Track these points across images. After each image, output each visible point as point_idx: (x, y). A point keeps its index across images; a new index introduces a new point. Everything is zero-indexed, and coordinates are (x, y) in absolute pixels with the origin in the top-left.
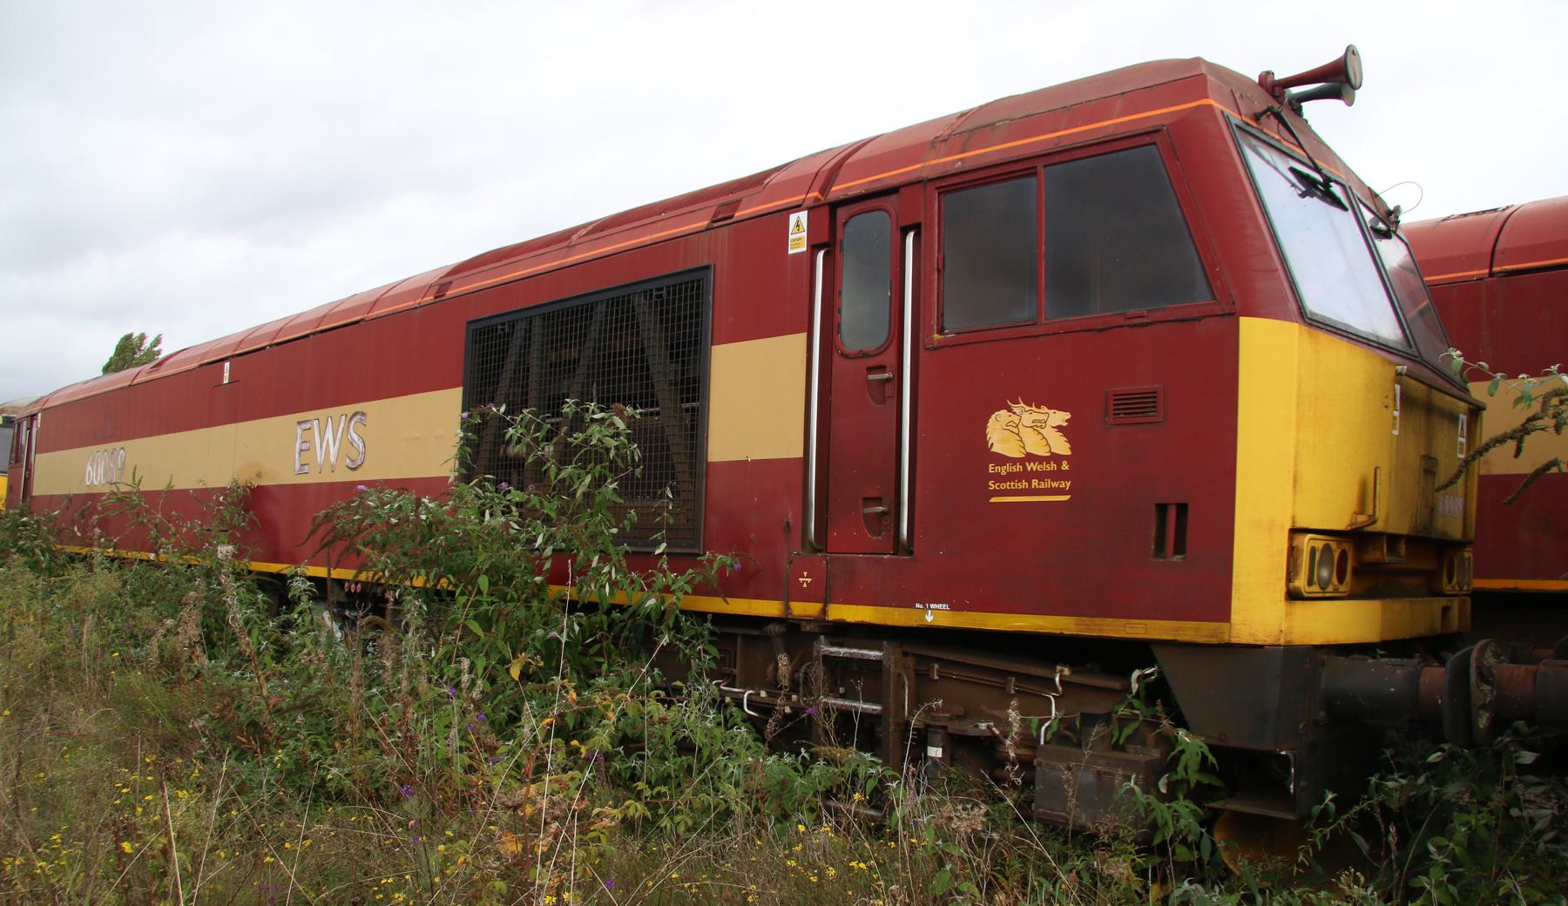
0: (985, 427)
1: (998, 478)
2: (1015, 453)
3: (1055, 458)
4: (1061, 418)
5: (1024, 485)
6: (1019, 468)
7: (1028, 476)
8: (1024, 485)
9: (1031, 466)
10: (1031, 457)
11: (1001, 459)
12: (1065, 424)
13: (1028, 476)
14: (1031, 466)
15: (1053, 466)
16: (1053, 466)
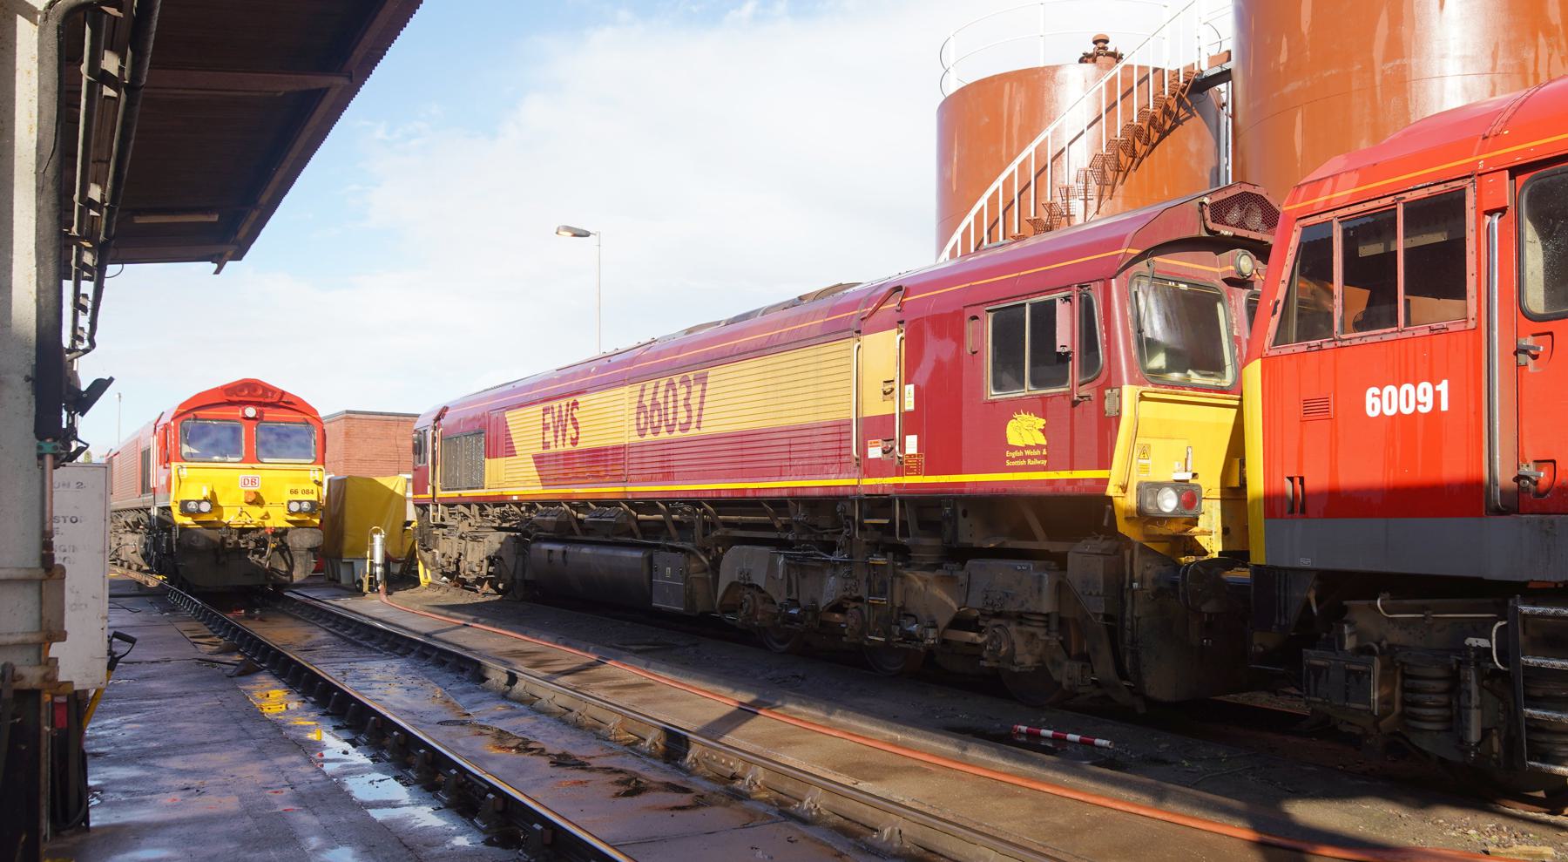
0: (1006, 427)
1: (1011, 459)
2: (1020, 443)
3: (1038, 447)
4: (1041, 422)
5: (1023, 463)
6: (1021, 453)
7: (1026, 457)
8: (1023, 463)
9: (1028, 452)
10: (1028, 447)
11: (1014, 448)
12: (1043, 427)
13: (1026, 457)
14: (1028, 452)
15: (1037, 453)
16: (1037, 453)
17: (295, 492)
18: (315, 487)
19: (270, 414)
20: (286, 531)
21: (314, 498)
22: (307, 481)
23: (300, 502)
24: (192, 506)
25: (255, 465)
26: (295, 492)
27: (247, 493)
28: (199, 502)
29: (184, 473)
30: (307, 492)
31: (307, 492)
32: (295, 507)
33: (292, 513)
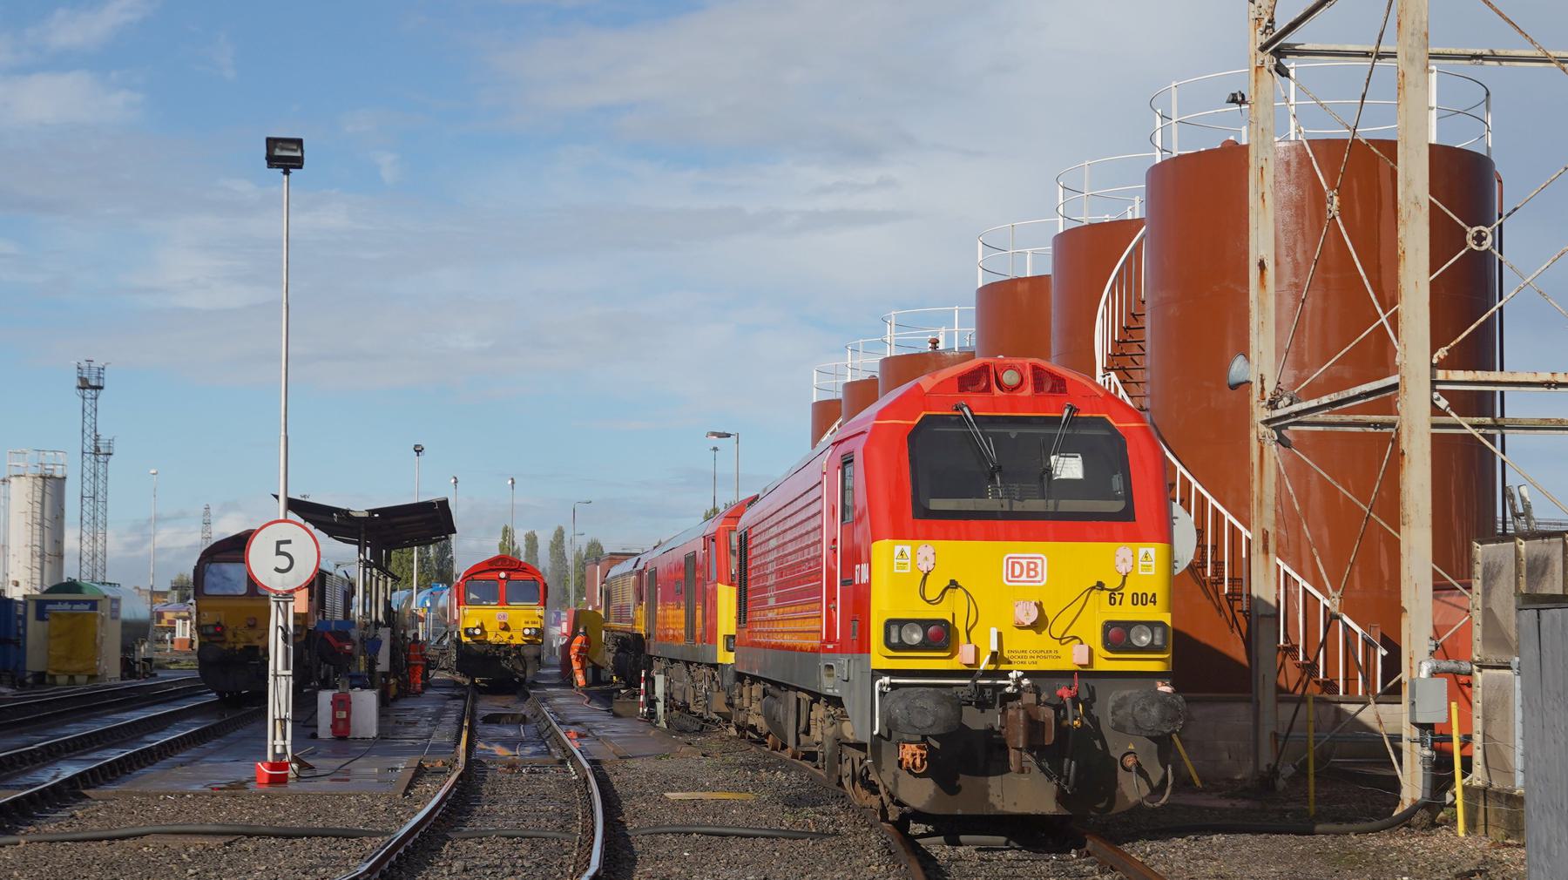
17: (527, 623)
18: (539, 620)
19: (514, 575)
20: (522, 645)
21: (538, 626)
22: (534, 616)
23: (530, 629)
24: (471, 631)
25: (506, 607)
26: (527, 623)
27: (501, 623)
28: (474, 629)
29: (467, 612)
30: (534, 623)
31: (534, 623)
32: (527, 632)
33: (525, 636)
